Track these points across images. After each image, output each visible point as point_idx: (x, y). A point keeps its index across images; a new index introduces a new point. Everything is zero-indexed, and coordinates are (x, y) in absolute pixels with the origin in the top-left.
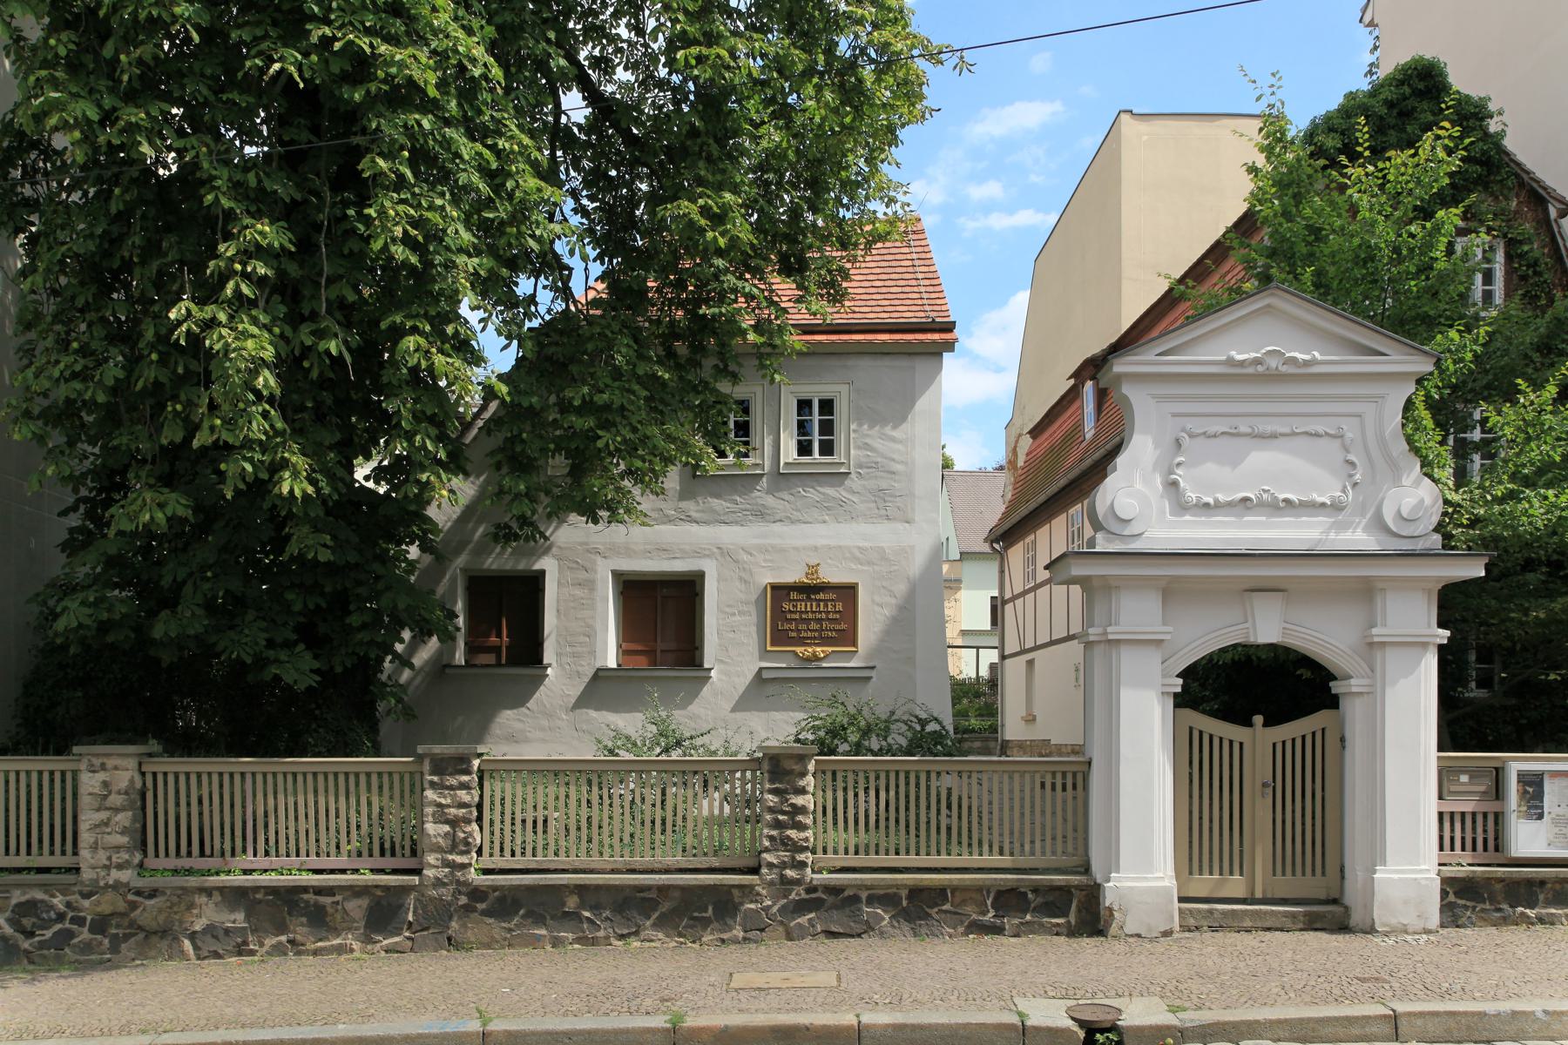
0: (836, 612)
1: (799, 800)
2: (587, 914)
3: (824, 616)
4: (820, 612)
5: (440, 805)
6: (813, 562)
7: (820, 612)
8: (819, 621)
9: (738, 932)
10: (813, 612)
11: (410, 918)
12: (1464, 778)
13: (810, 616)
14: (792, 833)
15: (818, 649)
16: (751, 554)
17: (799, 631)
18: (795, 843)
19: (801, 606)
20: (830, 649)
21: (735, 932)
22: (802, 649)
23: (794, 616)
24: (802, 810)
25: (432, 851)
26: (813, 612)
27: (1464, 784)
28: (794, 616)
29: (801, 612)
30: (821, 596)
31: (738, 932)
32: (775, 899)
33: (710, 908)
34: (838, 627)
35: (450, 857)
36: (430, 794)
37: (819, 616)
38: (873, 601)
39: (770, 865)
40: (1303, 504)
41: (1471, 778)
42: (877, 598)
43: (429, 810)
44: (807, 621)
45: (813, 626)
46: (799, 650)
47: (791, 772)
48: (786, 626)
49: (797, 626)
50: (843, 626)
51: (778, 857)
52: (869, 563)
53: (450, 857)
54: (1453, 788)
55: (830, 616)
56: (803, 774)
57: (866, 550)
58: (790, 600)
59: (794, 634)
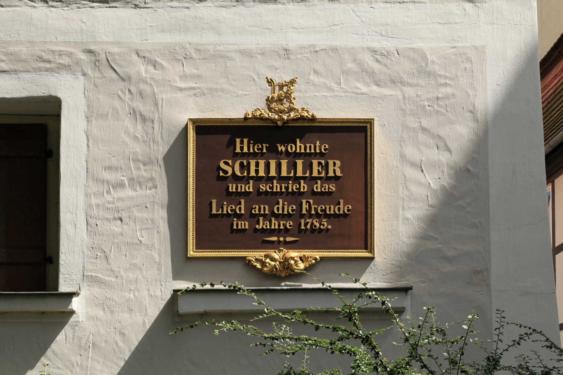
0: (328, 179)
3: (304, 187)
4: (297, 179)
10: (281, 179)
15: (294, 254)
16: (155, 65)
17: (254, 218)
20: (317, 254)
22: (259, 254)
23: (243, 188)
26: (281, 179)
28: (243, 188)
29: (258, 179)
30: (299, 146)
34: (332, 209)
37: (292, 187)
38: (402, 156)
42: (411, 152)
46: (253, 255)
48: (227, 209)
49: (249, 208)
50: (343, 208)
52: (395, 81)
55: (318, 187)
57: (386, 54)
58: (236, 156)
59: (244, 225)
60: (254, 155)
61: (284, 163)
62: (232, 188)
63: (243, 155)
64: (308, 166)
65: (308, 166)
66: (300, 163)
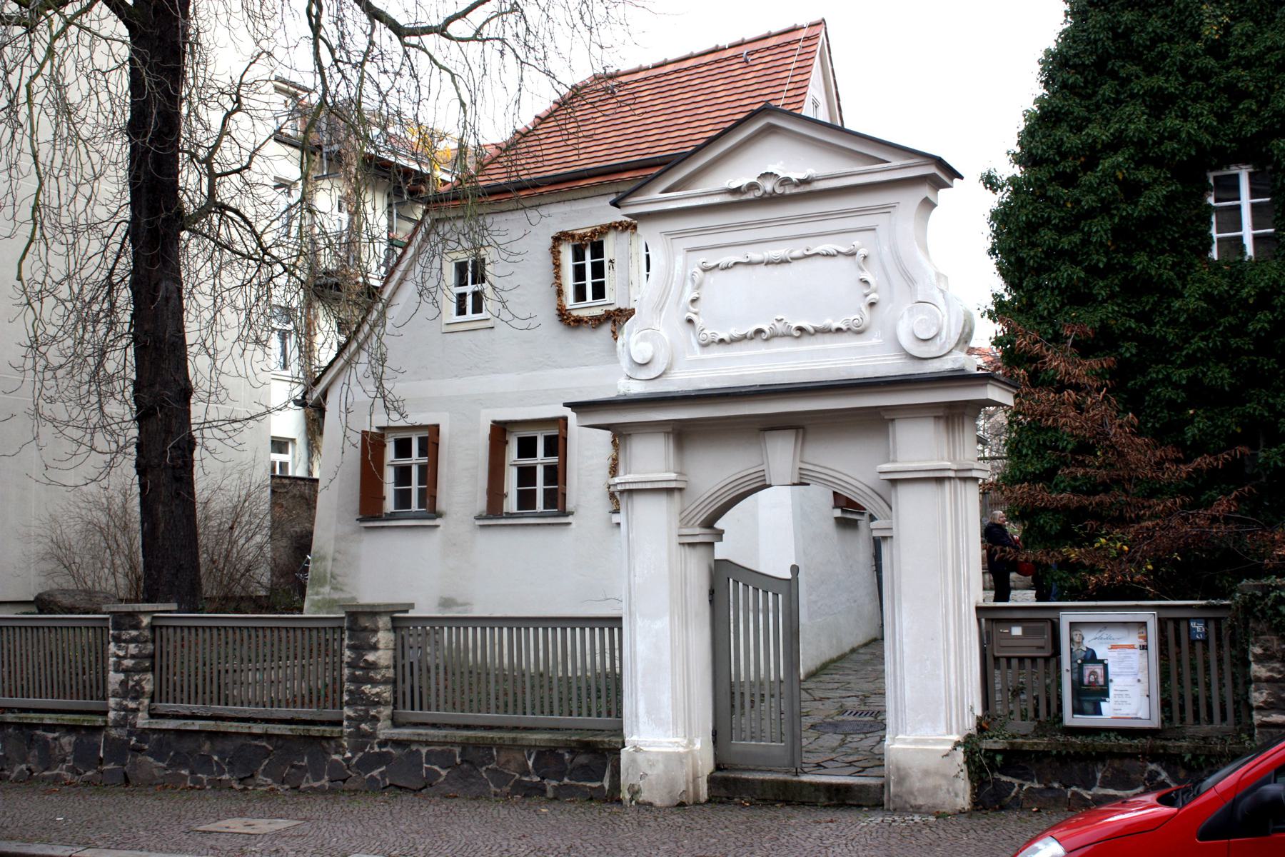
1: (371, 657)
2: (216, 758)
5: (118, 656)
9: (325, 782)
11: (101, 755)
12: (1017, 631)
14: (367, 688)
18: (368, 698)
21: (323, 782)
24: (373, 666)
25: (113, 696)
27: (1017, 637)
31: (325, 782)
32: (354, 753)
33: (306, 759)
35: (125, 703)
36: (112, 647)
39: (349, 718)
40: (819, 331)
41: (1024, 631)
43: (112, 660)
47: (365, 629)
51: (356, 711)
53: (125, 703)
54: (1004, 643)
56: (375, 631)
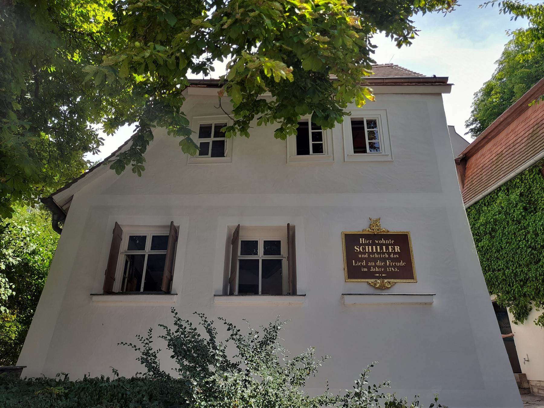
0: (395, 253)
4: (384, 253)
6: (374, 218)
7: (384, 253)
8: (384, 260)
10: (378, 253)
13: (376, 256)
17: (369, 268)
19: (368, 249)
29: (369, 253)
44: (375, 260)
45: (378, 263)
48: (359, 264)
49: (367, 263)
50: (402, 264)
55: (392, 256)
58: (360, 245)
60: (368, 245)
61: (378, 247)
62: (360, 256)
63: (362, 244)
64: (387, 248)
65: (387, 248)
66: (384, 247)
